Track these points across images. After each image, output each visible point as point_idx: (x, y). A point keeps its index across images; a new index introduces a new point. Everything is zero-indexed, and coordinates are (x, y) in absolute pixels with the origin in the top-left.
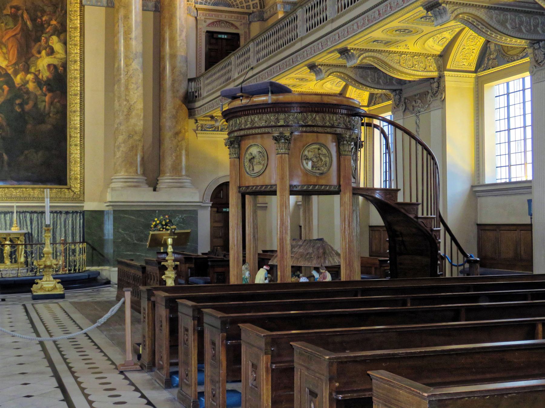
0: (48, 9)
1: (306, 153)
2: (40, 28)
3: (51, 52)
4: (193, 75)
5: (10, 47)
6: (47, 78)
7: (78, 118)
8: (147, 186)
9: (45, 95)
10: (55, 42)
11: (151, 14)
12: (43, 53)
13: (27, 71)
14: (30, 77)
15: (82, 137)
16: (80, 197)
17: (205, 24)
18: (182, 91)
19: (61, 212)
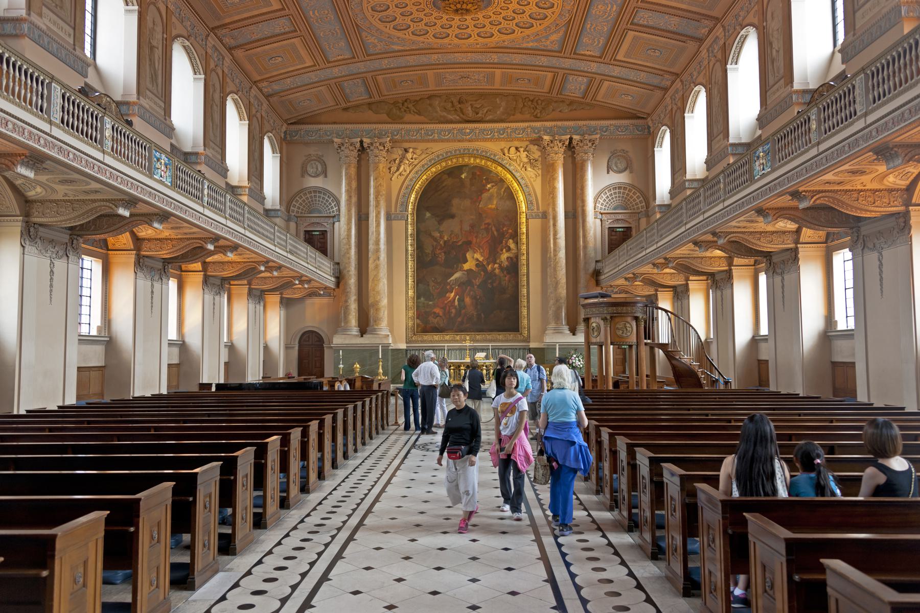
0: (507, 223)
1: (619, 326)
2: (502, 235)
3: (509, 249)
4: (599, 258)
5: (485, 248)
6: (507, 266)
7: (526, 290)
8: (569, 332)
9: (506, 276)
10: (511, 244)
11: (571, 220)
12: (504, 250)
13: (495, 263)
14: (496, 266)
15: (528, 302)
16: (527, 340)
17: (607, 223)
18: (591, 269)
19: (516, 349)
